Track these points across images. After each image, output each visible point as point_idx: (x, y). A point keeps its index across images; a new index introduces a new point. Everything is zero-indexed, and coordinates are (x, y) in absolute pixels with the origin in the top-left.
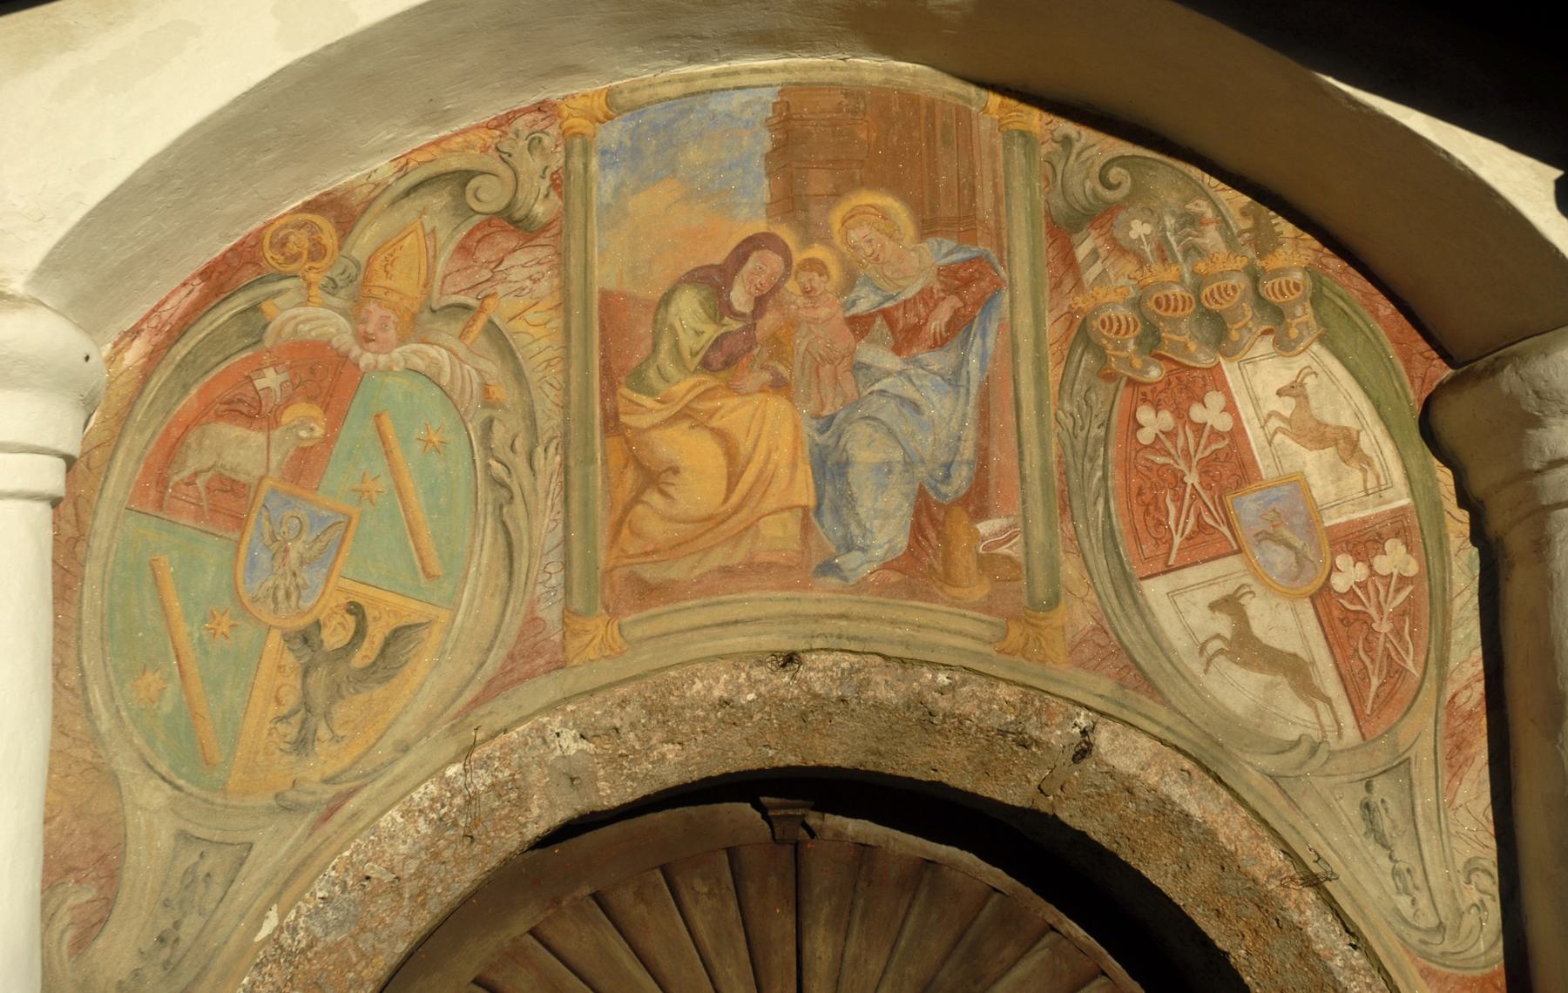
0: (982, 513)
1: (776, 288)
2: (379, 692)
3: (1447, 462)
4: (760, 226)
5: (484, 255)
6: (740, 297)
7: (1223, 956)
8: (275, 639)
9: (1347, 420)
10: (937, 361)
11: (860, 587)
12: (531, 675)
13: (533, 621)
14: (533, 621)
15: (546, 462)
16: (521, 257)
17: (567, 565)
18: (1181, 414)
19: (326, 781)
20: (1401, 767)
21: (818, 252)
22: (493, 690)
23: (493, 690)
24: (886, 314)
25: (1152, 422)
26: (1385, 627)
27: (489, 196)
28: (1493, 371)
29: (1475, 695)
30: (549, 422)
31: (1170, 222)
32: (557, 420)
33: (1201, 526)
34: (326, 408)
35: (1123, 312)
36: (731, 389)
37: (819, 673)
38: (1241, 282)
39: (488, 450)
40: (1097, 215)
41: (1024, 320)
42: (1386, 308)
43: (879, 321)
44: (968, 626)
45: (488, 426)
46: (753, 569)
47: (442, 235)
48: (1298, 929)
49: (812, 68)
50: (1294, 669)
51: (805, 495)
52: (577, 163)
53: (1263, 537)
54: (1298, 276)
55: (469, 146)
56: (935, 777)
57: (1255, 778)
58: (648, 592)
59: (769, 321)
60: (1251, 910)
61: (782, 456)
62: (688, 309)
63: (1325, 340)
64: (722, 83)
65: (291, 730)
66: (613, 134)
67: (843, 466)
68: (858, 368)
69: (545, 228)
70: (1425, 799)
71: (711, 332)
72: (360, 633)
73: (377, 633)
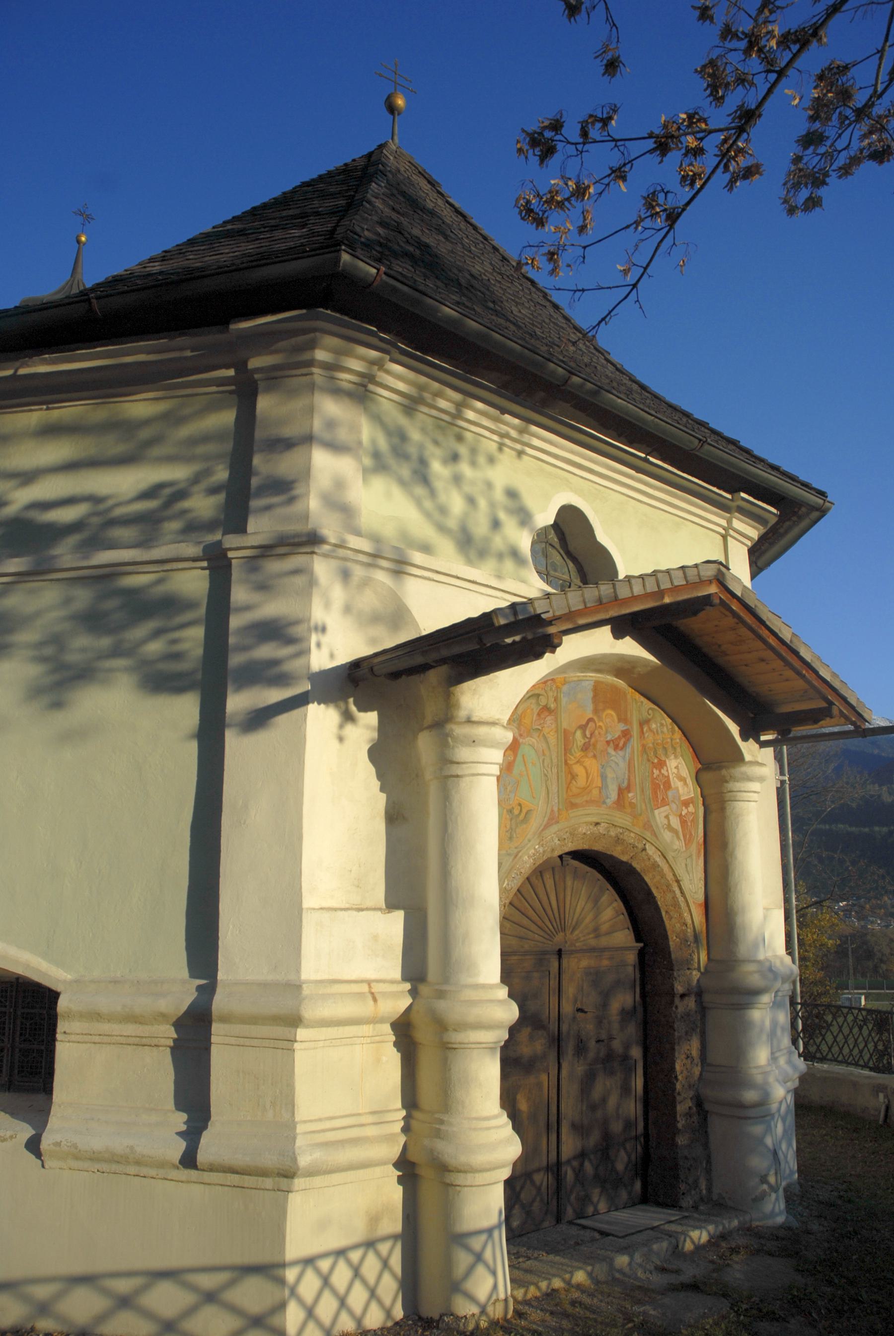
0: (629, 792)
1: (594, 732)
2: (525, 826)
3: (700, 787)
4: (591, 716)
5: (542, 716)
6: (588, 734)
7: (654, 898)
8: (505, 810)
9: (685, 776)
10: (621, 753)
11: (610, 807)
12: (552, 824)
13: (552, 811)
14: (552, 811)
15: (555, 770)
16: (549, 718)
17: (558, 797)
18: (660, 771)
19: (516, 848)
20: (691, 856)
21: (601, 724)
22: (547, 827)
23: (547, 827)
24: (613, 741)
25: (656, 772)
26: (689, 824)
27: (543, 701)
28: (720, 768)
29: (702, 840)
30: (555, 761)
31: (659, 725)
32: (556, 760)
33: (663, 798)
34: (513, 752)
35: (651, 745)
36: (586, 756)
37: (601, 829)
38: (669, 740)
39: (544, 767)
40: (648, 722)
41: (635, 745)
42: (691, 750)
43: (612, 743)
44: (627, 819)
45: (543, 761)
46: (589, 802)
47: (535, 710)
48: (674, 892)
49: (599, 677)
50: (675, 832)
51: (600, 785)
52: (559, 694)
53: (673, 801)
54: (678, 740)
55: (539, 687)
56: (612, 853)
57: (670, 857)
58: (573, 806)
59: (593, 740)
60: (665, 888)
61: (595, 774)
62: (579, 734)
63: (682, 756)
64: (584, 678)
65: (508, 834)
66: (565, 688)
67: (606, 777)
68: (608, 753)
69: (553, 711)
70: (694, 862)
71: (583, 741)
72: (521, 811)
73: (524, 811)
